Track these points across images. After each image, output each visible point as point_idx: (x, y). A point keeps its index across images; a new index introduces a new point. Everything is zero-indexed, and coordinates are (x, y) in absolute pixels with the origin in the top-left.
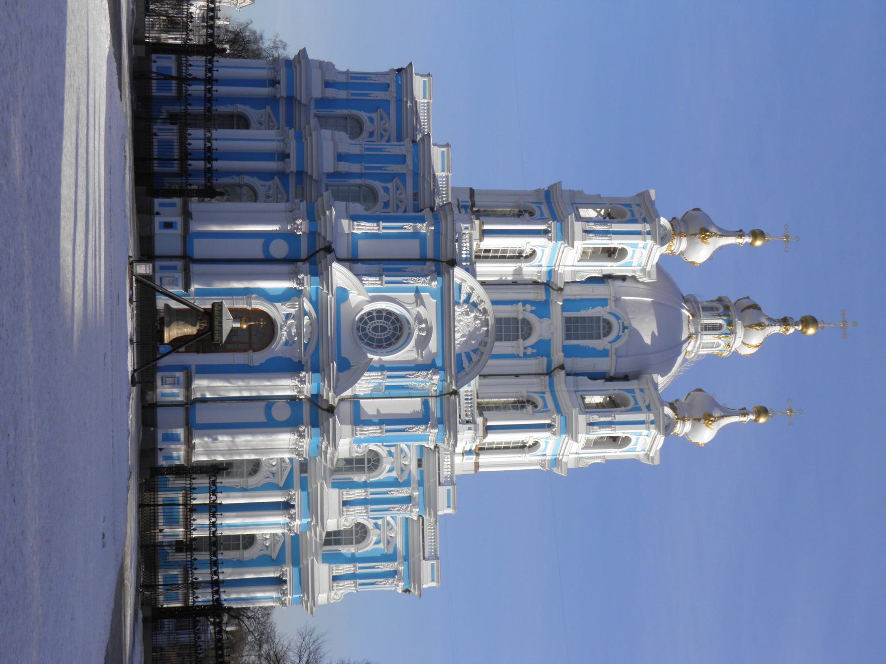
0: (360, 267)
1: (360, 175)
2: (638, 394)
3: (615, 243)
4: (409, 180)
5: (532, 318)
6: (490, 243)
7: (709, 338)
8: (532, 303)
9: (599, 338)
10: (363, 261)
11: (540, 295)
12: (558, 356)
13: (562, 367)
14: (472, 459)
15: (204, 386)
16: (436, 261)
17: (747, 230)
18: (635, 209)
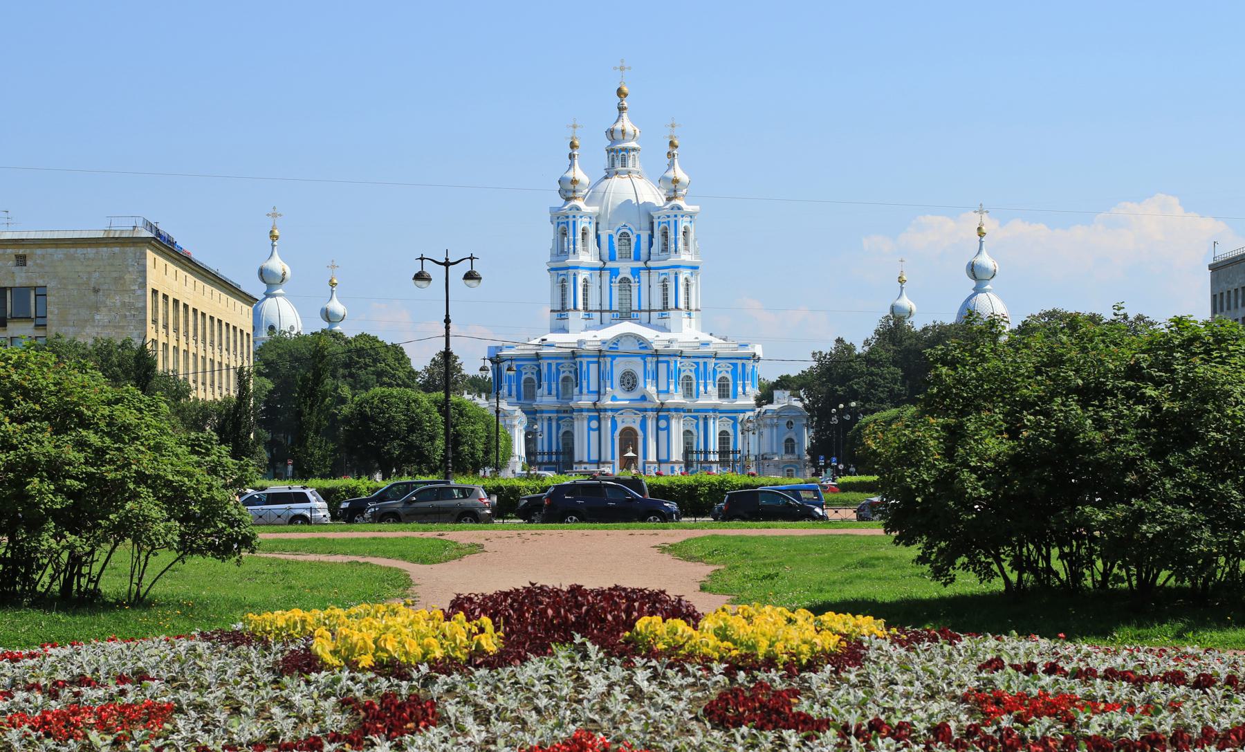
0: (602, 391)
1: (557, 384)
2: (661, 220)
3: (579, 236)
4: (559, 361)
5: (619, 277)
6: (580, 306)
7: (630, 162)
8: (611, 278)
9: (629, 240)
10: (599, 388)
11: (606, 275)
12: (641, 264)
13: (645, 263)
14: (694, 314)
15: (652, 457)
16: (599, 357)
17: (570, 151)
18: (560, 221)
